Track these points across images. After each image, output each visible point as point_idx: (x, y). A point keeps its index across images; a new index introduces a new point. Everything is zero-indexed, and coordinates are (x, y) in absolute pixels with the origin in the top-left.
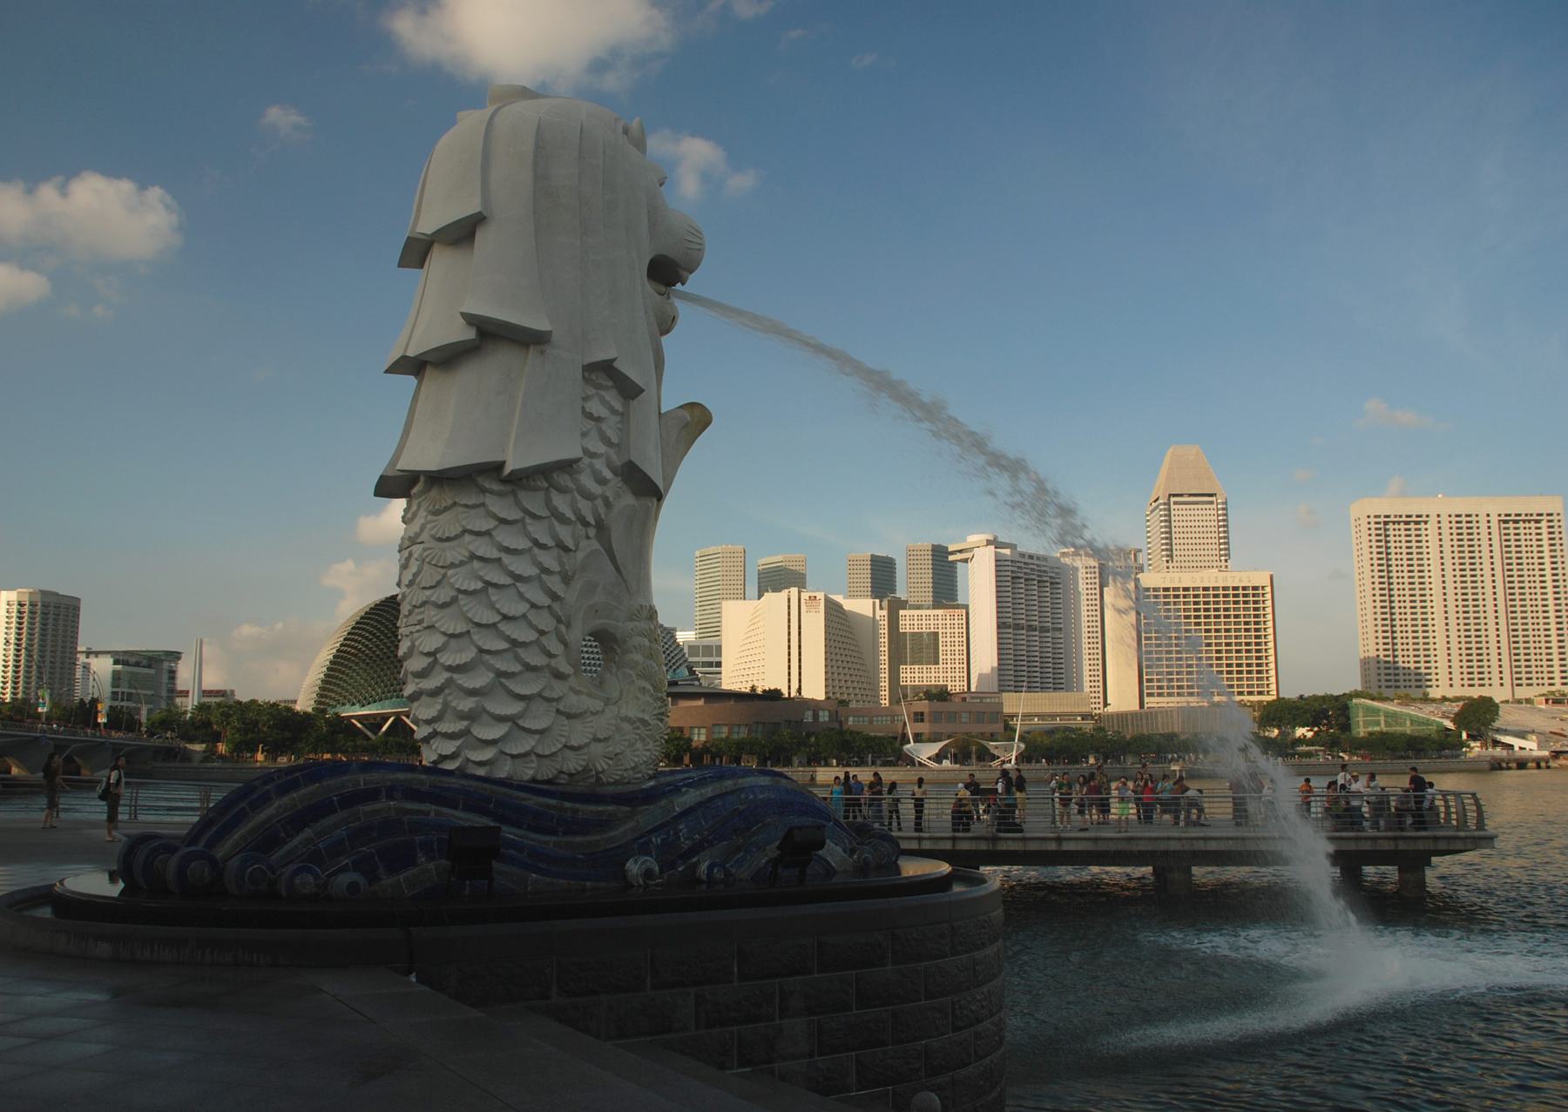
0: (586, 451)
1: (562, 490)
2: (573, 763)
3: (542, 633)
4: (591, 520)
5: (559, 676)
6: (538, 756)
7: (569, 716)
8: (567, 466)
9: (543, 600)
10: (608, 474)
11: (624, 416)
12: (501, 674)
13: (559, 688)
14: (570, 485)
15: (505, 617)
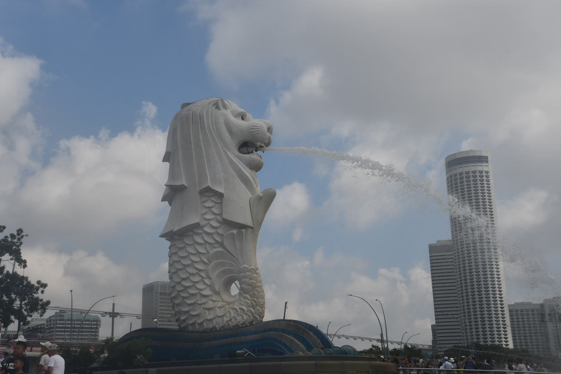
0: (206, 219)
1: (198, 234)
2: (211, 326)
3: (195, 282)
4: (211, 241)
5: (206, 296)
6: (199, 324)
7: (209, 309)
8: (197, 226)
9: (195, 271)
10: (215, 224)
11: (222, 203)
12: (184, 298)
13: (204, 300)
14: (201, 232)
15: (184, 279)
